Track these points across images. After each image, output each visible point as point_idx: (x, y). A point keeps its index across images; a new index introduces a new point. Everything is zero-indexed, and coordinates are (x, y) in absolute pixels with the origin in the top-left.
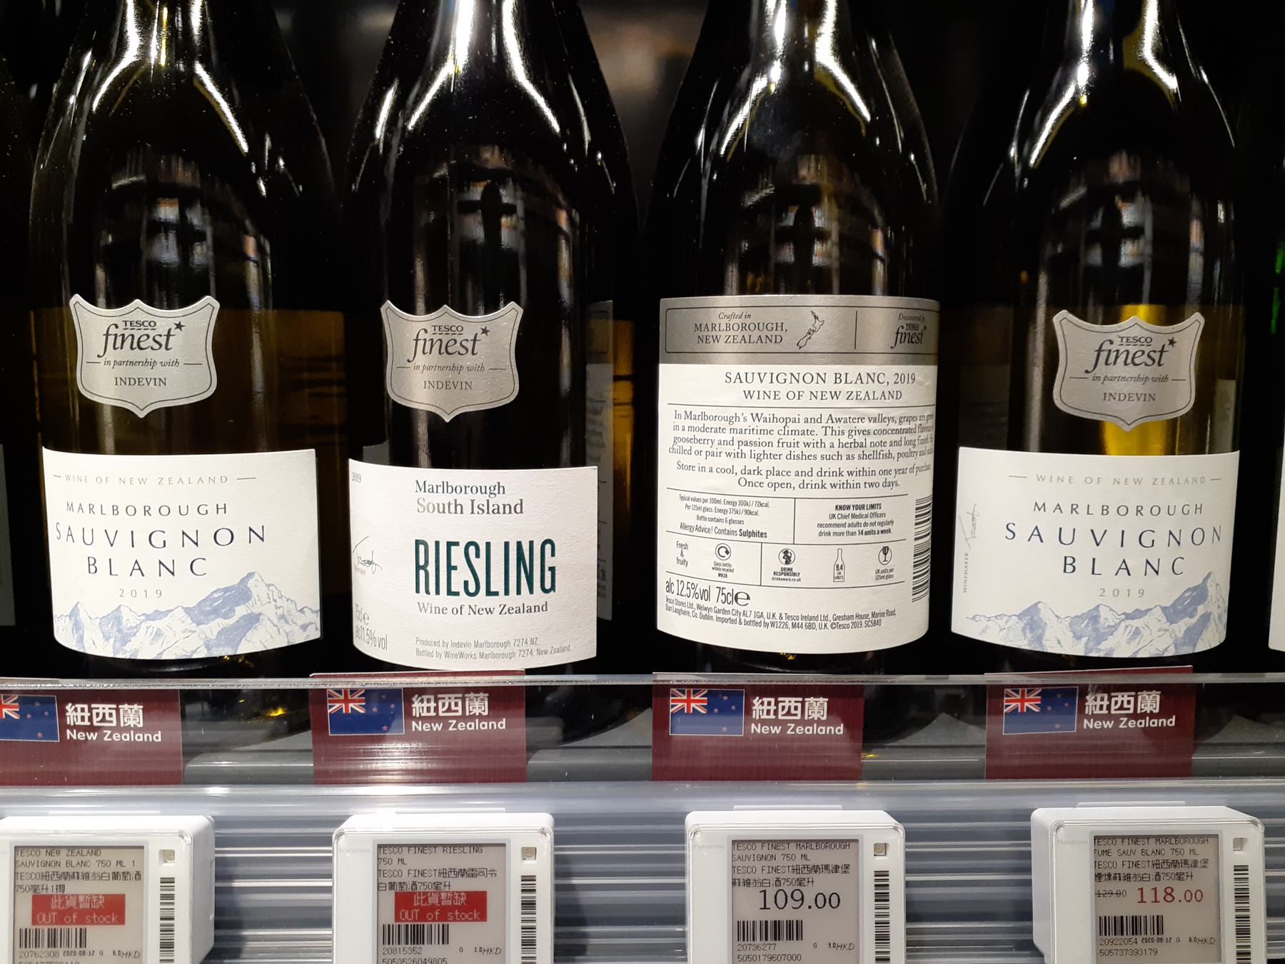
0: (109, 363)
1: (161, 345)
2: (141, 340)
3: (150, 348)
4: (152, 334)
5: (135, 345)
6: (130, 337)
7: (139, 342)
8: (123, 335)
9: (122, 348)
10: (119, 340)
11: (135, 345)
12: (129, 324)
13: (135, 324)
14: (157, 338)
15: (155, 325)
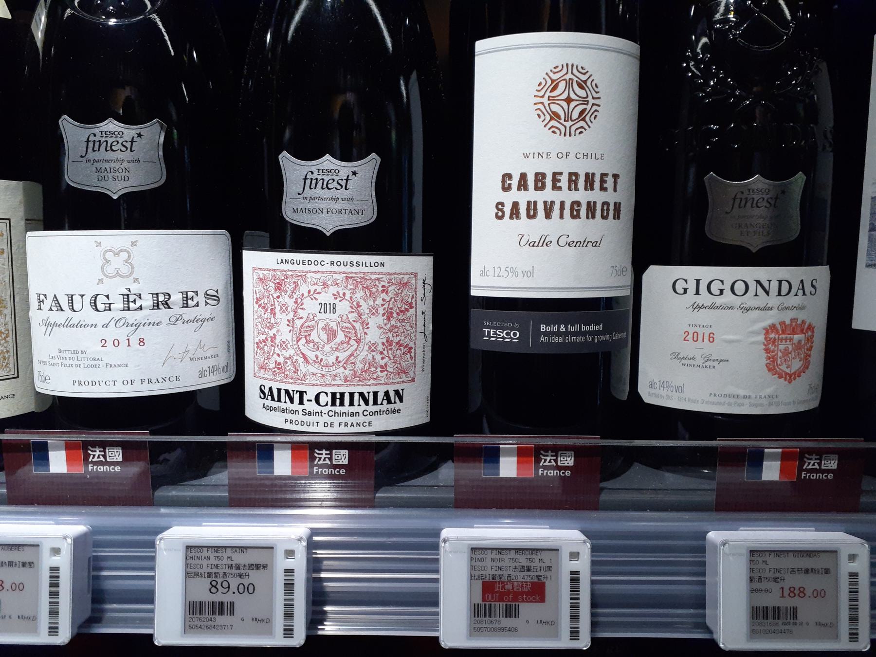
0: (89, 161)
1: (127, 148)
2: (113, 144)
3: (119, 150)
4: (120, 140)
5: (109, 148)
6: (105, 143)
7: (111, 146)
8: (100, 141)
9: (99, 150)
10: (97, 144)
11: (109, 148)
12: (103, 133)
13: (109, 134)
14: (124, 143)
15: (123, 134)
